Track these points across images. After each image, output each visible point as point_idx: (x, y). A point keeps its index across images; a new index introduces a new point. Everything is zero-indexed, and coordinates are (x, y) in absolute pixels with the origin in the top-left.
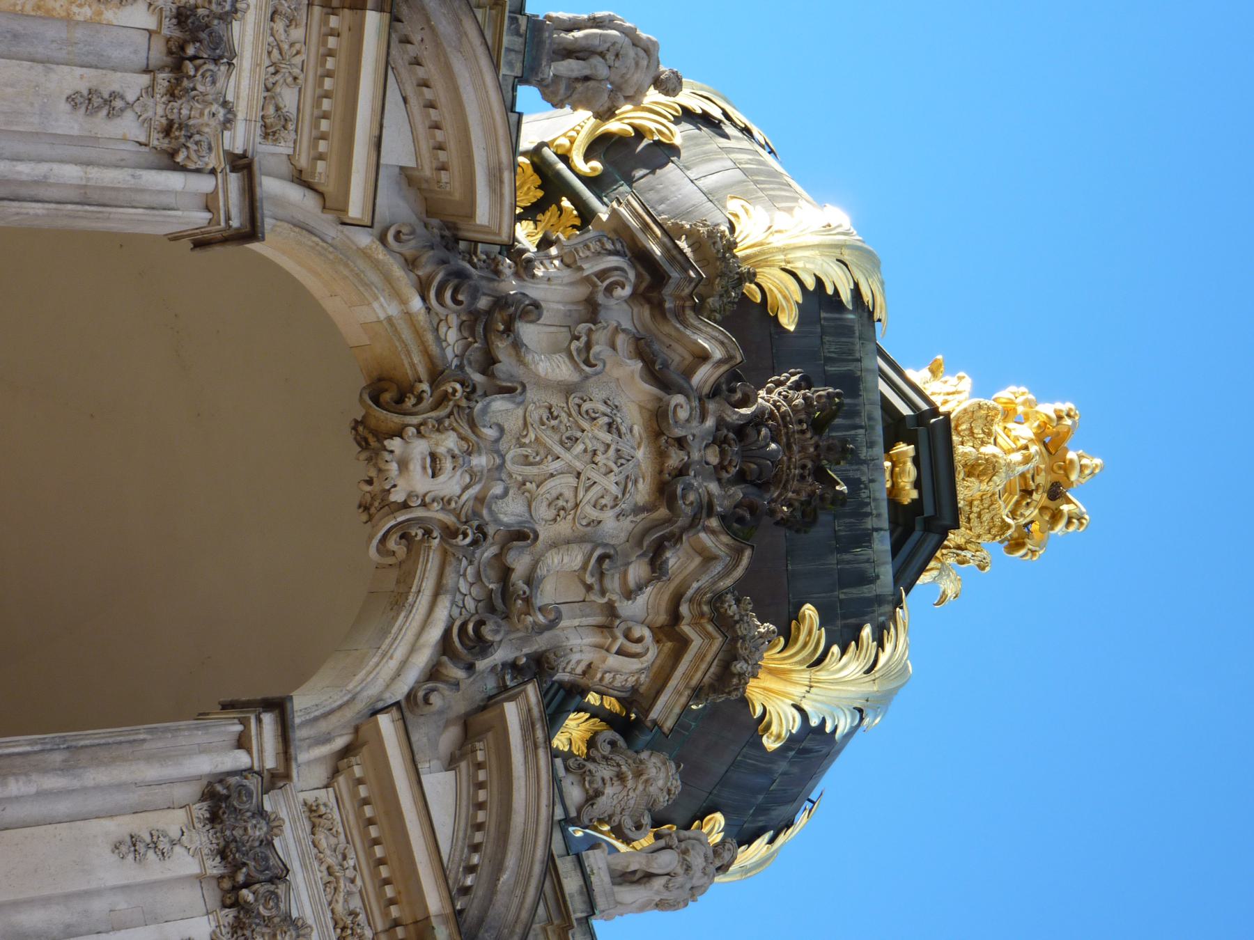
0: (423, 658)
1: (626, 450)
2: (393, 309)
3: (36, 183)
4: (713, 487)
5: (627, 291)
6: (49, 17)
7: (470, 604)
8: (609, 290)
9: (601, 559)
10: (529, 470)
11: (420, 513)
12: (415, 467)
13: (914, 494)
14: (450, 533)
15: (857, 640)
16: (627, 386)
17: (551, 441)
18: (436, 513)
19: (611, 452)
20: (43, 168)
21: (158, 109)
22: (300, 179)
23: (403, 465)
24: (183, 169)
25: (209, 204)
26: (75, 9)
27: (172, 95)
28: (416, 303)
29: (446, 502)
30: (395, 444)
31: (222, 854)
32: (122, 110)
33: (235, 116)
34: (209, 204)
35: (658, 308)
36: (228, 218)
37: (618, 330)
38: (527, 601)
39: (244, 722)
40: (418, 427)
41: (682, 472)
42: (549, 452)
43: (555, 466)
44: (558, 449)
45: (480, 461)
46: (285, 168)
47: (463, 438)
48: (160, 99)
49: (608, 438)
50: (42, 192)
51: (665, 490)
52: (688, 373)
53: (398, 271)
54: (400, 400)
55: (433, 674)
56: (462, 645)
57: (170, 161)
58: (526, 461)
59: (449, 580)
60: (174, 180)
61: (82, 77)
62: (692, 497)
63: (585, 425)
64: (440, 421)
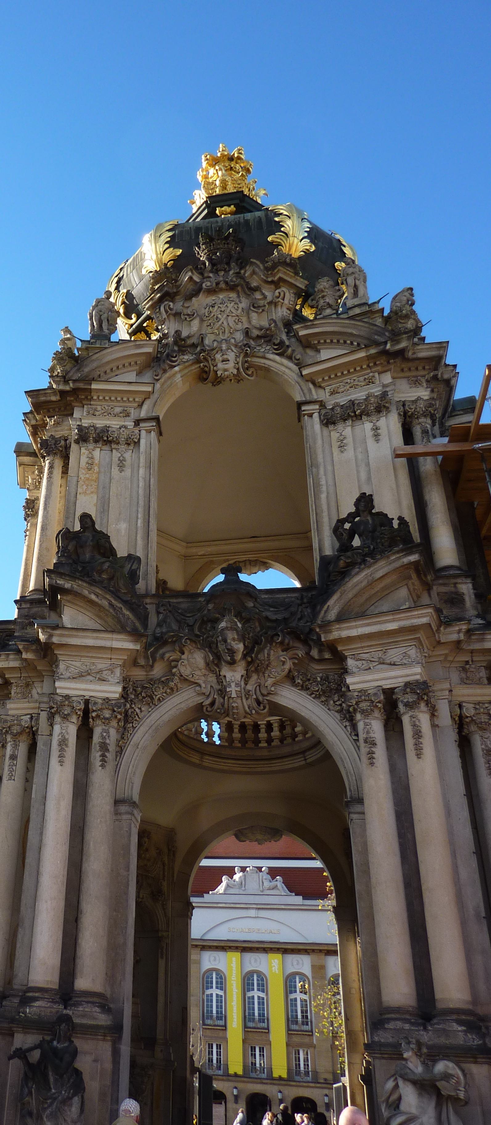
0: (285, 362)
1: (220, 301)
2: (179, 376)
3: (145, 481)
4: (231, 272)
5: (171, 304)
6: (98, 478)
7: (268, 348)
8: (171, 309)
9: (254, 307)
11: (240, 364)
12: (226, 366)
14: (246, 355)
16: (200, 302)
18: (240, 360)
19: (221, 306)
20: (140, 479)
21: (123, 447)
22: (141, 405)
23: (226, 370)
24: (139, 440)
25: (149, 432)
27: (118, 443)
28: (177, 369)
29: (237, 357)
34: (149, 432)
35: (176, 294)
36: (153, 426)
37: (183, 306)
38: (267, 330)
39: (304, 415)
40: (214, 366)
41: (226, 283)
42: (221, 325)
43: (225, 324)
44: (220, 323)
45: (224, 346)
47: (217, 352)
49: (216, 307)
50: (148, 479)
51: (232, 288)
52: (196, 283)
53: (167, 375)
54: (206, 372)
56: (281, 349)
57: (137, 443)
58: (224, 332)
59: (260, 354)
60: (143, 442)
62: (234, 279)
63: (212, 315)
64: (212, 360)
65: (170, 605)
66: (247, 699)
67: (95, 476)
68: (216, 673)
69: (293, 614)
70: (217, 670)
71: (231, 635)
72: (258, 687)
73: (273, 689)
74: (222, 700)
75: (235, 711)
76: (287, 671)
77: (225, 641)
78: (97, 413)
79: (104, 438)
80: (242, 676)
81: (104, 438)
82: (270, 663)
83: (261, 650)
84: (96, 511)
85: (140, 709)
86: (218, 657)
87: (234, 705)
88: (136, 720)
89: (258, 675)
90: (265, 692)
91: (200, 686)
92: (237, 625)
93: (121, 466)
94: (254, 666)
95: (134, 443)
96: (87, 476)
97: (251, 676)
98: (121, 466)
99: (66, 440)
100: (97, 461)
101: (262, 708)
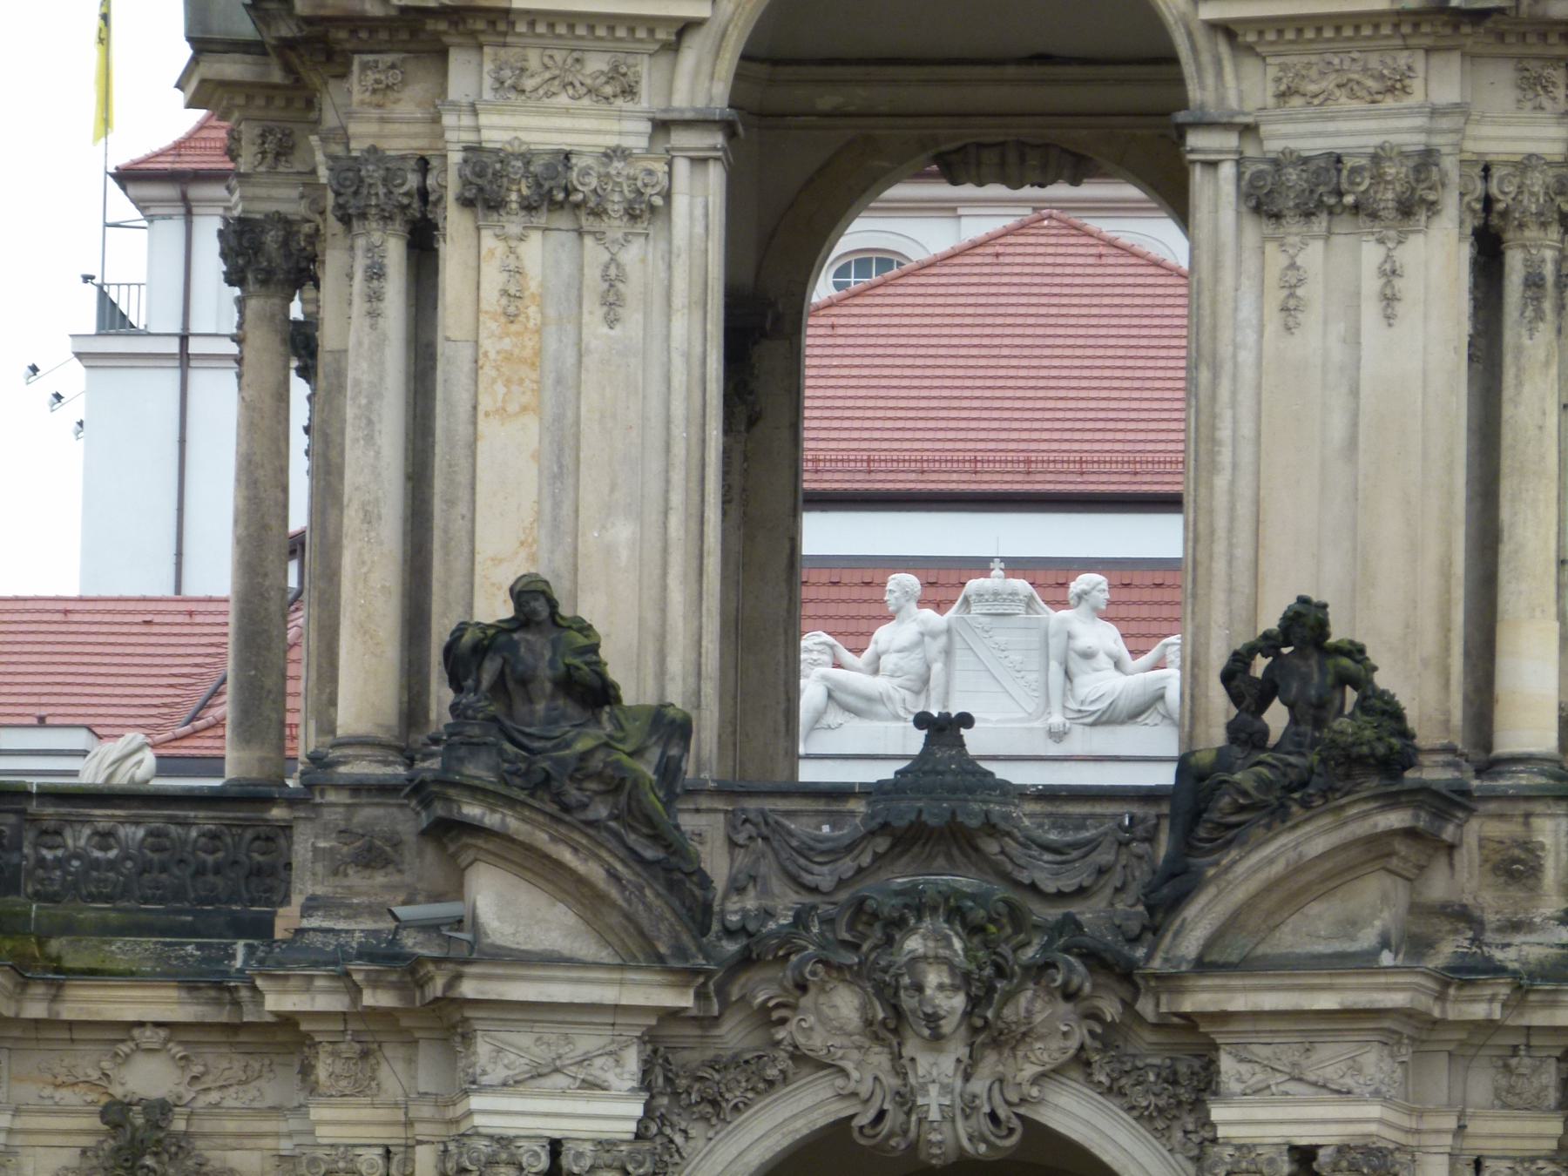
6: (539, 352)
20: (678, 363)
21: (615, 227)
24: (667, 196)
26: (531, 324)
27: (598, 213)
31: (1308, 215)
32: (618, 266)
33: (618, 147)
34: (699, 162)
46: (663, 61)
48: (602, 225)
50: (698, 349)
60: (680, 203)
61: (591, 313)
65: (767, 823)
66: (967, 1117)
67: (530, 343)
68: (890, 1046)
69: (1102, 871)
70: (895, 1043)
71: (934, 977)
72: (996, 1086)
73: (1035, 1092)
74: (902, 1118)
75: (936, 1151)
76: (1072, 1052)
77: (919, 988)
78: (529, 84)
80: (959, 1061)
81: (552, 192)
82: (1031, 1030)
83: (1009, 997)
84: (540, 472)
85: (685, 1132)
86: (897, 1011)
87: (935, 1137)
88: (677, 1164)
89: (1000, 1054)
90: (1014, 1098)
91: (843, 1072)
92: (950, 945)
93: (612, 304)
94: (988, 1033)
95: (647, 210)
96: (507, 343)
97: (982, 1058)
98: (612, 304)
99: (424, 165)
100: (533, 286)
101: (1004, 1133)
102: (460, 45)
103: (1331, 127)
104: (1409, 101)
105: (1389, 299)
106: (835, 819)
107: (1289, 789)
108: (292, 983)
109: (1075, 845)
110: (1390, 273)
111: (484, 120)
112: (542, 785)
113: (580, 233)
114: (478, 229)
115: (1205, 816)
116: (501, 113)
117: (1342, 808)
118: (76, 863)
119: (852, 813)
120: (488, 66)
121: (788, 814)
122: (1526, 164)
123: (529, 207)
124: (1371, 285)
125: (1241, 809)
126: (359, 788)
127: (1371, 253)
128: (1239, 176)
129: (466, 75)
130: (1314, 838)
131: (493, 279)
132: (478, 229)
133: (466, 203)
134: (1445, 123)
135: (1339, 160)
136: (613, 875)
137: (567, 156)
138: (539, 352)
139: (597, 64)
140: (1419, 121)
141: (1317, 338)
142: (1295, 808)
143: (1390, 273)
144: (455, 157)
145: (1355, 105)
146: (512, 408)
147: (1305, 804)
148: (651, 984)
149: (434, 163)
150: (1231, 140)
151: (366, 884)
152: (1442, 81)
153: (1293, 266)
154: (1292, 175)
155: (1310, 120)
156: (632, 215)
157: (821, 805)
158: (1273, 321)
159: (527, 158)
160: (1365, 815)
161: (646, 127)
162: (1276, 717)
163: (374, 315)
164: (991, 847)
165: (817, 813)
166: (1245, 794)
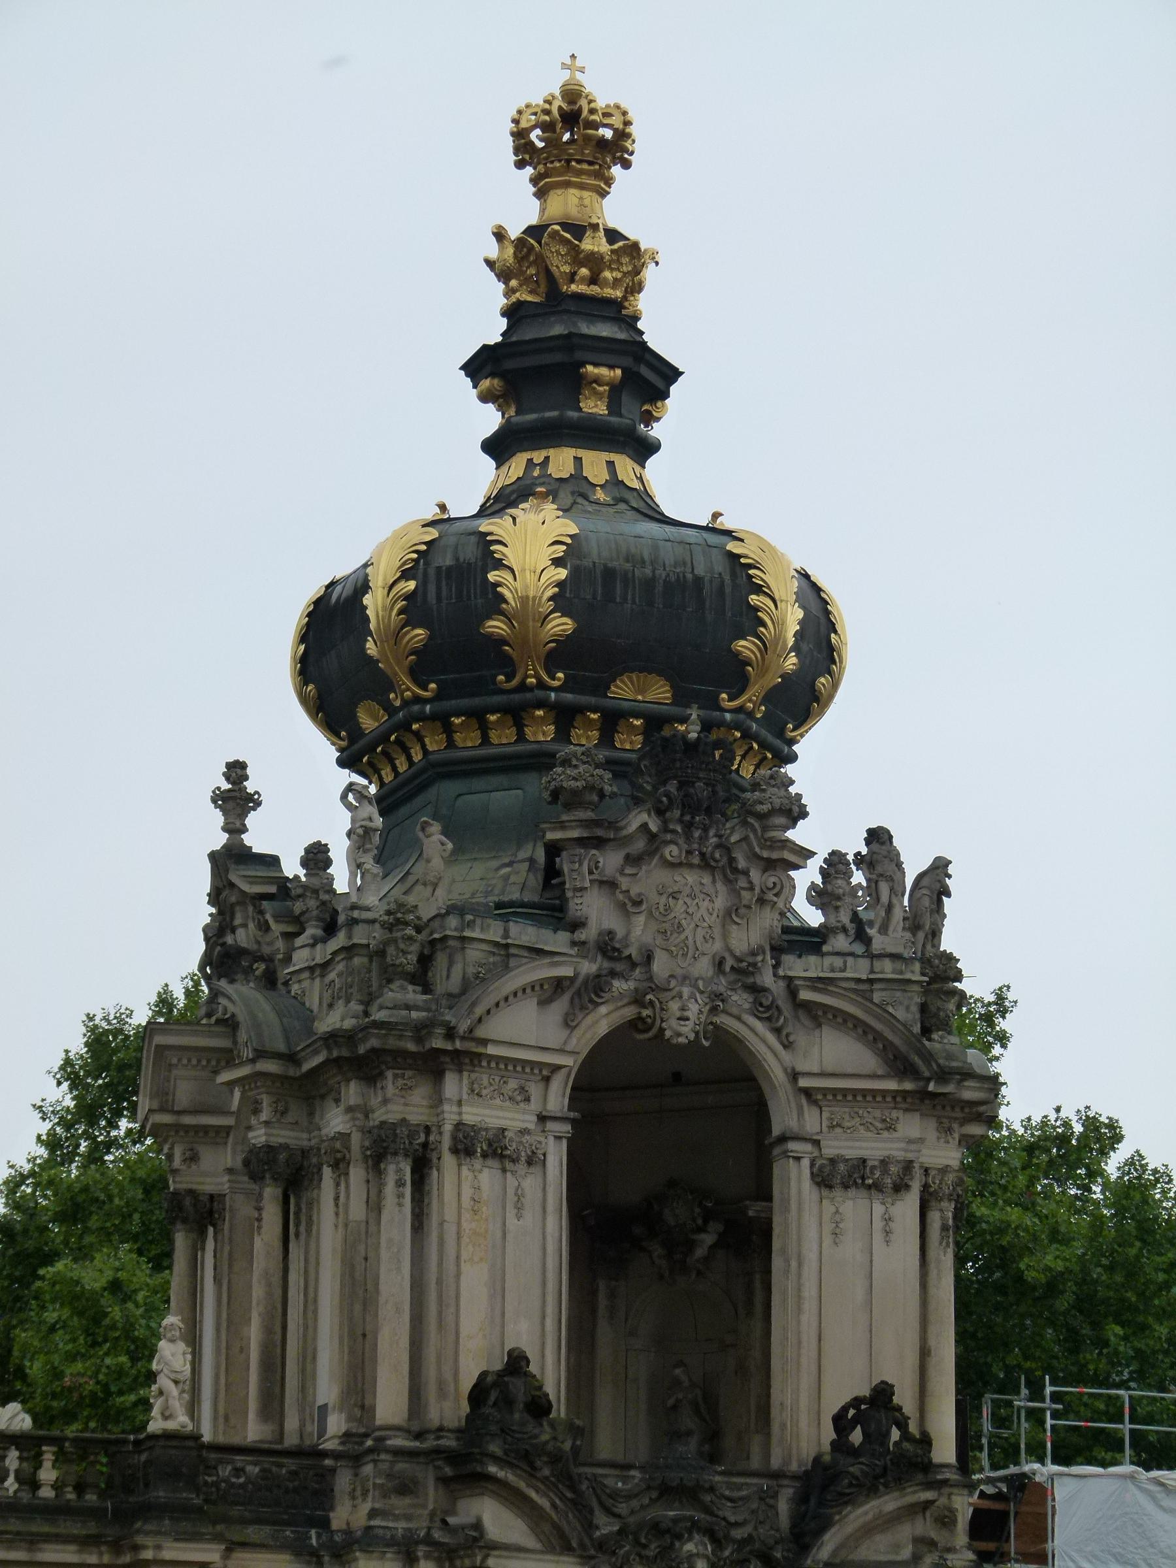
0: (771, 1038)
1: (687, 890)
10: (690, 955)
13: (619, 372)
14: (714, 1010)
15: (757, 609)
17: (676, 939)
21: (521, 1168)
27: (514, 1161)
30: (668, 1034)
31: (846, 1187)
34: (558, 1138)
40: (662, 1021)
41: (702, 855)
42: (684, 941)
44: (683, 937)
45: (686, 991)
47: (673, 998)
49: (681, 902)
55: (777, 1031)
58: (685, 955)
63: (673, 915)
79: (495, 1149)
81: (495, 1149)
93: (519, 1208)
95: (535, 1160)
98: (519, 1208)
99: (428, 1130)
102: (450, 1070)
103: (857, 1144)
104: (895, 1135)
105: (887, 1233)
106: (625, 1479)
107: (876, 1478)
108: (375, 1555)
109: (741, 1499)
110: (888, 1219)
111: (465, 1109)
112: (524, 1458)
113: (504, 1170)
114: (460, 1165)
115: (832, 1488)
116: (472, 1106)
117: (904, 1488)
118: (223, 1485)
119: (633, 1477)
120: (465, 1081)
121: (606, 1476)
122: (944, 1170)
123: (485, 1156)
124: (878, 1224)
125: (851, 1485)
126: (398, 1453)
127: (878, 1209)
128: (812, 1165)
129: (452, 1085)
130: (889, 1503)
131: (467, 1192)
132: (460, 1165)
133: (455, 1151)
134: (913, 1147)
135: (864, 1161)
136: (554, 1506)
137: (504, 1130)
138: (486, 1231)
139: (513, 1084)
140: (903, 1145)
141: (851, 1249)
142: (881, 1487)
143: (888, 1219)
144: (448, 1128)
145: (870, 1134)
146: (476, 1259)
147: (886, 1486)
148: (568, 1562)
149: (434, 1129)
150: (808, 1147)
151: (400, 1503)
152: (912, 1126)
153: (837, 1212)
154: (842, 1167)
155: (846, 1140)
156: (530, 1163)
157: (617, 1472)
158: (827, 1240)
159: (486, 1129)
160: (915, 1492)
161: (535, 1119)
162: (857, 1436)
163: (400, 1205)
164: (708, 1498)
165: (617, 1476)
166: (857, 1478)
